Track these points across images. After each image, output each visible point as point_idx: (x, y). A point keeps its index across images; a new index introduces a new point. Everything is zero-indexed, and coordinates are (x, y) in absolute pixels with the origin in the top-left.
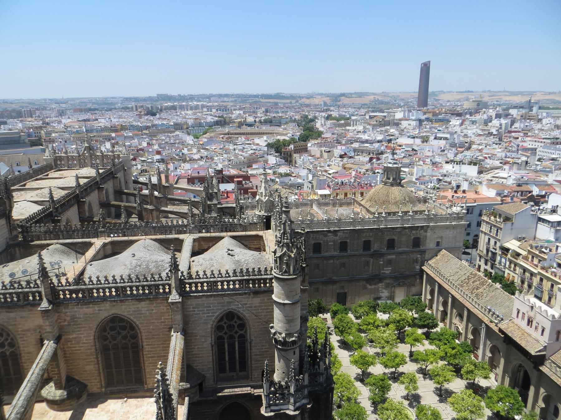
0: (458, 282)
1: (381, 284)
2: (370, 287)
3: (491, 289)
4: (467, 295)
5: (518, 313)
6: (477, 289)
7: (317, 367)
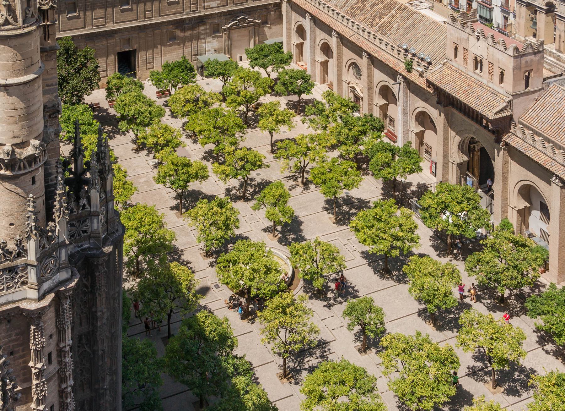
0: (346, 8)
1: (202, 28)
2: (181, 35)
3: (405, 15)
4: (364, 30)
5: (456, 49)
6: (380, 18)
7: (85, 201)
